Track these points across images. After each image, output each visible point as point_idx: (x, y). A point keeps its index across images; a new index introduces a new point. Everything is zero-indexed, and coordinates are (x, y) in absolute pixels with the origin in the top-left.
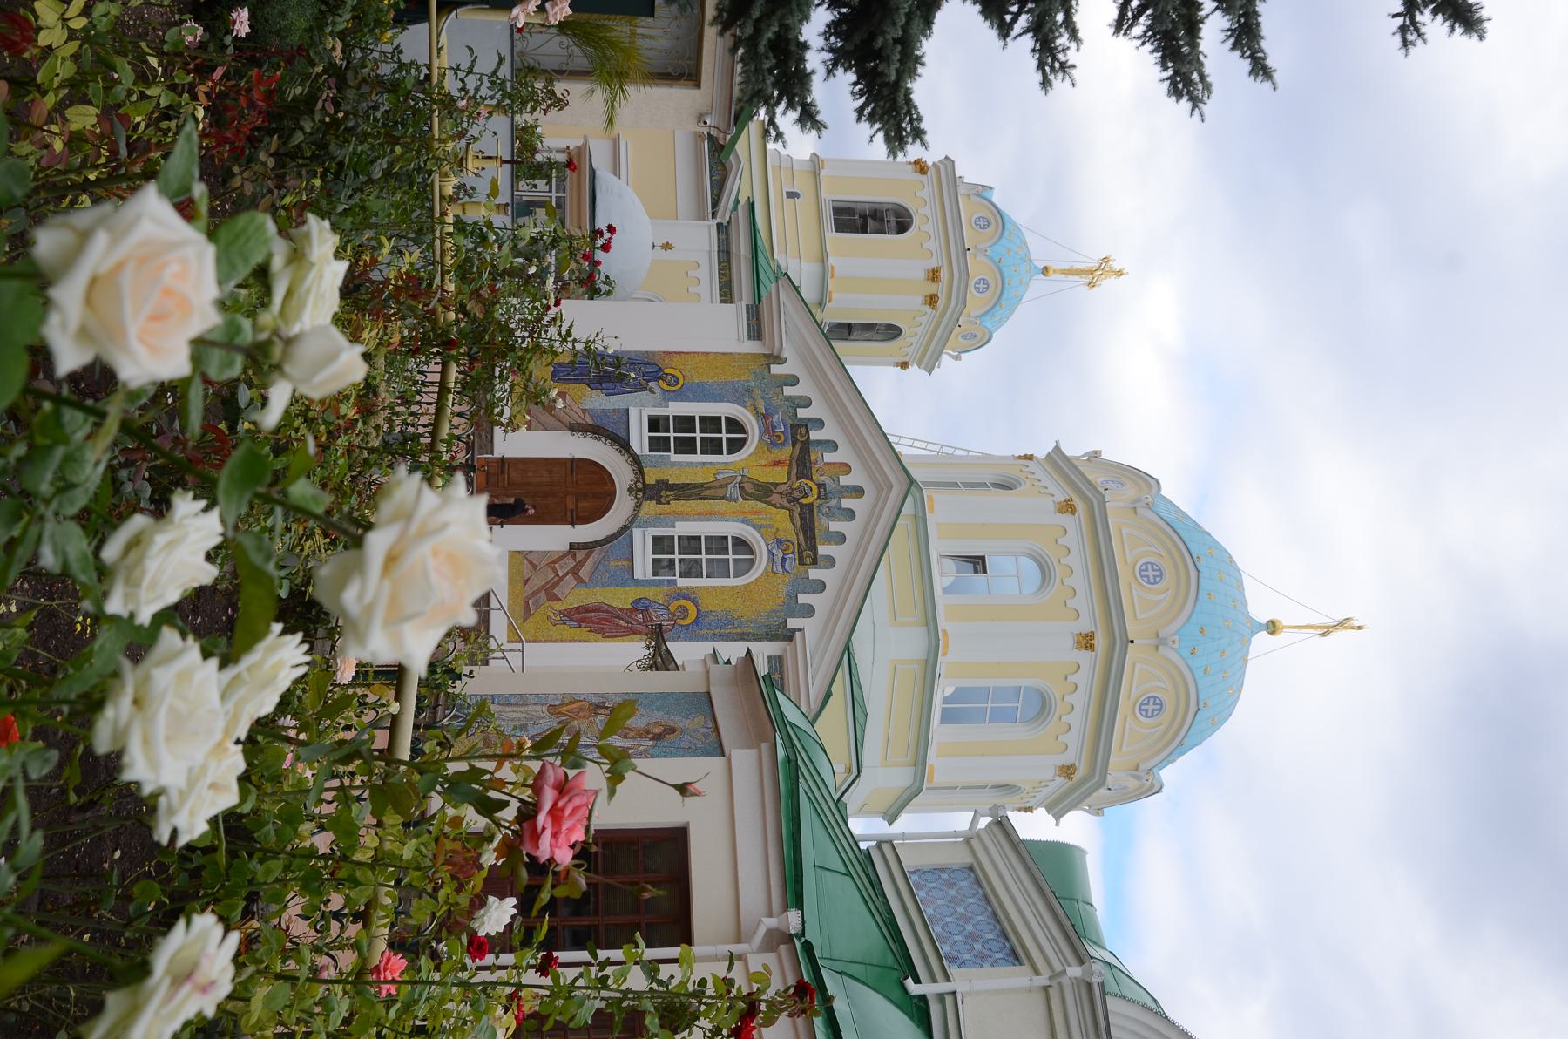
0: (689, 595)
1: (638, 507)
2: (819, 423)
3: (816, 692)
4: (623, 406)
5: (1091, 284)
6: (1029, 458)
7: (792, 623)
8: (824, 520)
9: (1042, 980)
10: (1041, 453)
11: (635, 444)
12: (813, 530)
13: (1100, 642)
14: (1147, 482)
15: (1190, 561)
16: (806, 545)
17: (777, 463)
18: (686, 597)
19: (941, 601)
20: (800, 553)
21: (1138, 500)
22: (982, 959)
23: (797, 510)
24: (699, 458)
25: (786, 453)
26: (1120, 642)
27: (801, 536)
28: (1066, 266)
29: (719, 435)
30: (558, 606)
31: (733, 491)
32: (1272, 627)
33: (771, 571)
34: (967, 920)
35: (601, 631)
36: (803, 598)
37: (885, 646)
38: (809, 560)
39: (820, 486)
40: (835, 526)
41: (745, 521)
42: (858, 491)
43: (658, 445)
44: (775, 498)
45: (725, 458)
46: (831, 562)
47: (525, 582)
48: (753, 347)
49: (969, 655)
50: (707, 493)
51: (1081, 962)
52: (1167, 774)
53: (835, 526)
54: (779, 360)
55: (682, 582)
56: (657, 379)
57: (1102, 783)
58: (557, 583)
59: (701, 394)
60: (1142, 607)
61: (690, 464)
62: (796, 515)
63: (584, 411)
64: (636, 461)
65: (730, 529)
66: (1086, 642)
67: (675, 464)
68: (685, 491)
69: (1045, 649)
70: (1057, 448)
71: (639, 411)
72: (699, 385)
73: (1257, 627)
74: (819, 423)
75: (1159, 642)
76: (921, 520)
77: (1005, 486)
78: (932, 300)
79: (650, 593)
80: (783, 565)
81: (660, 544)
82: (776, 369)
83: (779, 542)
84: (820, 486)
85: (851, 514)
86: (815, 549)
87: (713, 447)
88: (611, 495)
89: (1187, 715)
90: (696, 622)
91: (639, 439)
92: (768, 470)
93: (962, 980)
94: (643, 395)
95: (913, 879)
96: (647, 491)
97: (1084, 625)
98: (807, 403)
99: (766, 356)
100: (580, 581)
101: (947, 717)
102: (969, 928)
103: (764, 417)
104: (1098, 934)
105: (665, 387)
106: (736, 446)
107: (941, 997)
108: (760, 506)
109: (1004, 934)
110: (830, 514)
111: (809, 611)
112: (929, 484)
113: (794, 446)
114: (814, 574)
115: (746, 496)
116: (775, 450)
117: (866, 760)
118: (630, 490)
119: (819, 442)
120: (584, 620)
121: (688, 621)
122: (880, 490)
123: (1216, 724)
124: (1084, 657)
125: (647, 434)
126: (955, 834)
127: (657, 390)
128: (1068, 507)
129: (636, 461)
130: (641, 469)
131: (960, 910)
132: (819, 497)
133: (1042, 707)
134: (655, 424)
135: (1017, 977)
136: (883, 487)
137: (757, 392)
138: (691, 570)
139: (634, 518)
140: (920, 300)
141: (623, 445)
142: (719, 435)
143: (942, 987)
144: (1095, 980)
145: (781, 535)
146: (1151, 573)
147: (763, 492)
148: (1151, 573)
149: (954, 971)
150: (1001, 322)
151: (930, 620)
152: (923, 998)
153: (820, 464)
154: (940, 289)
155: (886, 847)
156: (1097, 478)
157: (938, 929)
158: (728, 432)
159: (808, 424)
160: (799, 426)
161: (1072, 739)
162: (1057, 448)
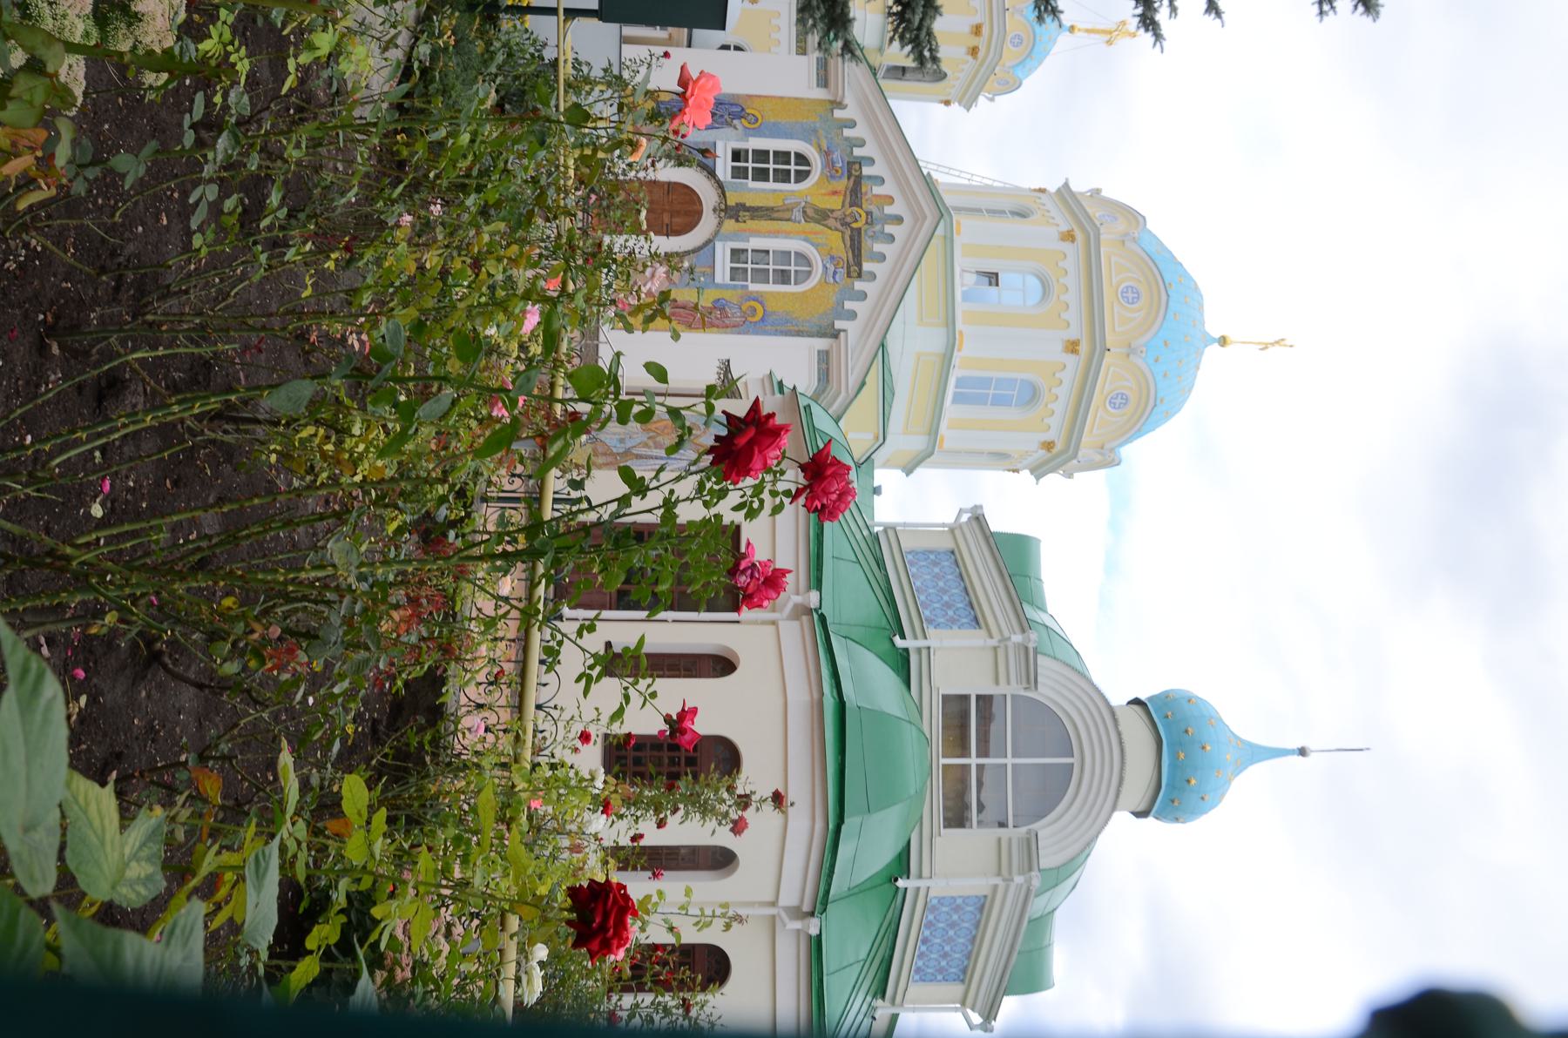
0: (758, 298)
1: (720, 224)
2: (871, 161)
3: (853, 380)
5: (1109, 42)
6: (1042, 191)
7: (839, 324)
8: (869, 242)
9: (994, 642)
10: (1052, 188)
11: (719, 173)
12: (860, 250)
13: (1084, 348)
14: (1134, 217)
15: (1161, 286)
16: (854, 262)
17: (835, 193)
19: (961, 307)
21: (1127, 234)
22: (952, 622)
24: (771, 185)
25: (843, 184)
26: (1099, 349)
28: (1089, 26)
29: (789, 167)
31: (797, 214)
32: (1223, 341)
34: (945, 591)
36: (848, 305)
37: (913, 341)
40: (878, 247)
41: (806, 240)
42: (899, 220)
43: (739, 173)
44: (831, 222)
45: (791, 186)
46: (873, 276)
48: (820, 94)
49: (978, 350)
50: (775, 215)
51: (1023, 631)
52: (1128, 451)
53: (878, 247)
54: (839, 105)
55: (753, 287)
57: (1075, 456)
59: (776, 132)
60: (1119, 321)
61: (764, 190)
64: (720, 186)
65: (793, 245)
66: (1072, 347)
67: (751, 190)
68: (757, 212)
69: (1040, 351)
70: (1066, 185)
73: (1208, 340)
74: (871, 161)
75: (1131, 351)
76: (949, 240)
77: (1022, 214)
78: (974, 51)
79: (727, 295)
81: (736, 254)
82: (838, 114)
83: (832, 258)
84: (869, 213)
85: (891, 238)
86: (860, 265)
87: (783, 176)
88: (700, 213)
89: (1145, 409)
90: (763, 320)
91: (724, 167)
93: (938, 639)
94: (728, 131)
95: (909, 558)
96: (731, 211)
97: (1073, 333)
98: (862, 143)
99: (832, 102)
101: (958, 399)
102: (946, 598)
103: (826, 154)
104: (1044, 603)
106: (802, 176)
107: (919, 650)
108: (819, 228)
109: (971, 605)
110: (874, 237)
111: (852, 315)
112: (959, 209)
114: (859, 285)
117: (891, 428)
118: (714, 210)
119: (870, 177)
121: (757, 318)
122: (916, 220)
123: (1168, 415)
124: (1070, 360)
125: (730, 164)
126: (944, 525)
128: (1069, 237)
129: (720, 186)
130: (724, 193)
131: (941, 584)
133: (1032, 395)
134: (737, 155)
135: (976, 638)
136: (919, 218)
137: (821, 132)
138: (761, 276)
139: (716, 233)
140: (963, 50)
141: (711, 173)
142: (789, 167)
143: (921, 643)
144: (1031, 646)
145: (834, 253)
146: (1130, 295)
147: (822, 216)
148: (1130, 295)
149: (930, 631)
150: (1031, 71)
151: (950, 322)
152: (906, 650)
154: (981, 42)
155: (891, 533)
156: (1095, 212)
157: (923, 598)
159: (860, 162)
161: (1054, 422)
162: (1066, 185)
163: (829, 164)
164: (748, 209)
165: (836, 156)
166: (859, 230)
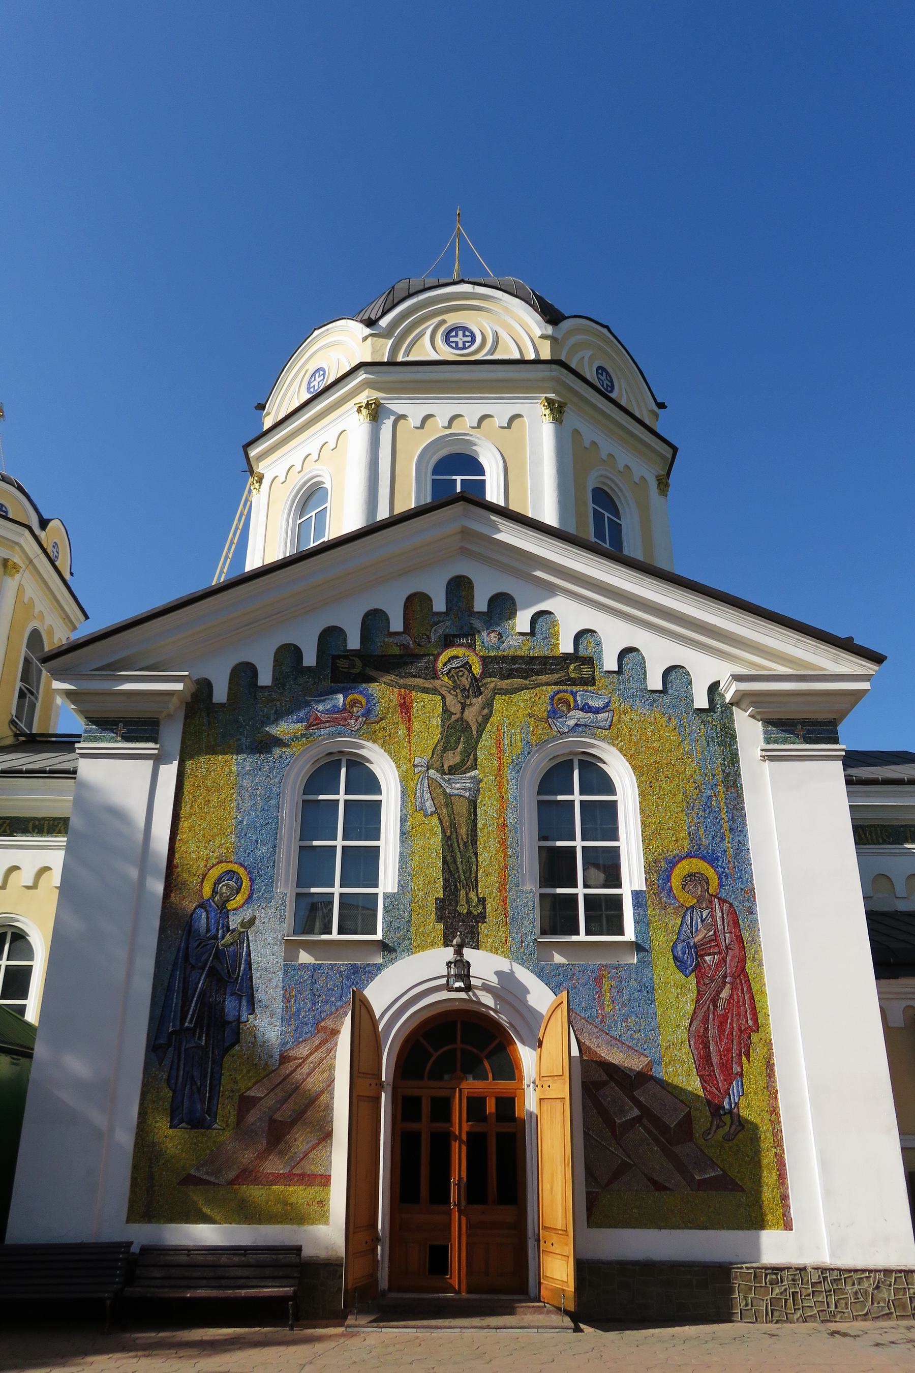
0: (659, 869)
17: (405, 707)
20: (573, 682)
23: (493, 682)
27: (543, 678)
31: (458, 786)
38: (586, 669)
44: (471, 715)
47: (659, 1187)
58: (656, 1121)
62: (505, 684)
80: (597, 711)
83: (554, 714)
90: (711, 860)
92: (416, 725)
105: (240, 898)
115: (469, 762)
120: (726, 1067)
121: (711, 873)
127: (247, 914)
145: (543, 708)
153: (408, 640)
166: (485, 660)
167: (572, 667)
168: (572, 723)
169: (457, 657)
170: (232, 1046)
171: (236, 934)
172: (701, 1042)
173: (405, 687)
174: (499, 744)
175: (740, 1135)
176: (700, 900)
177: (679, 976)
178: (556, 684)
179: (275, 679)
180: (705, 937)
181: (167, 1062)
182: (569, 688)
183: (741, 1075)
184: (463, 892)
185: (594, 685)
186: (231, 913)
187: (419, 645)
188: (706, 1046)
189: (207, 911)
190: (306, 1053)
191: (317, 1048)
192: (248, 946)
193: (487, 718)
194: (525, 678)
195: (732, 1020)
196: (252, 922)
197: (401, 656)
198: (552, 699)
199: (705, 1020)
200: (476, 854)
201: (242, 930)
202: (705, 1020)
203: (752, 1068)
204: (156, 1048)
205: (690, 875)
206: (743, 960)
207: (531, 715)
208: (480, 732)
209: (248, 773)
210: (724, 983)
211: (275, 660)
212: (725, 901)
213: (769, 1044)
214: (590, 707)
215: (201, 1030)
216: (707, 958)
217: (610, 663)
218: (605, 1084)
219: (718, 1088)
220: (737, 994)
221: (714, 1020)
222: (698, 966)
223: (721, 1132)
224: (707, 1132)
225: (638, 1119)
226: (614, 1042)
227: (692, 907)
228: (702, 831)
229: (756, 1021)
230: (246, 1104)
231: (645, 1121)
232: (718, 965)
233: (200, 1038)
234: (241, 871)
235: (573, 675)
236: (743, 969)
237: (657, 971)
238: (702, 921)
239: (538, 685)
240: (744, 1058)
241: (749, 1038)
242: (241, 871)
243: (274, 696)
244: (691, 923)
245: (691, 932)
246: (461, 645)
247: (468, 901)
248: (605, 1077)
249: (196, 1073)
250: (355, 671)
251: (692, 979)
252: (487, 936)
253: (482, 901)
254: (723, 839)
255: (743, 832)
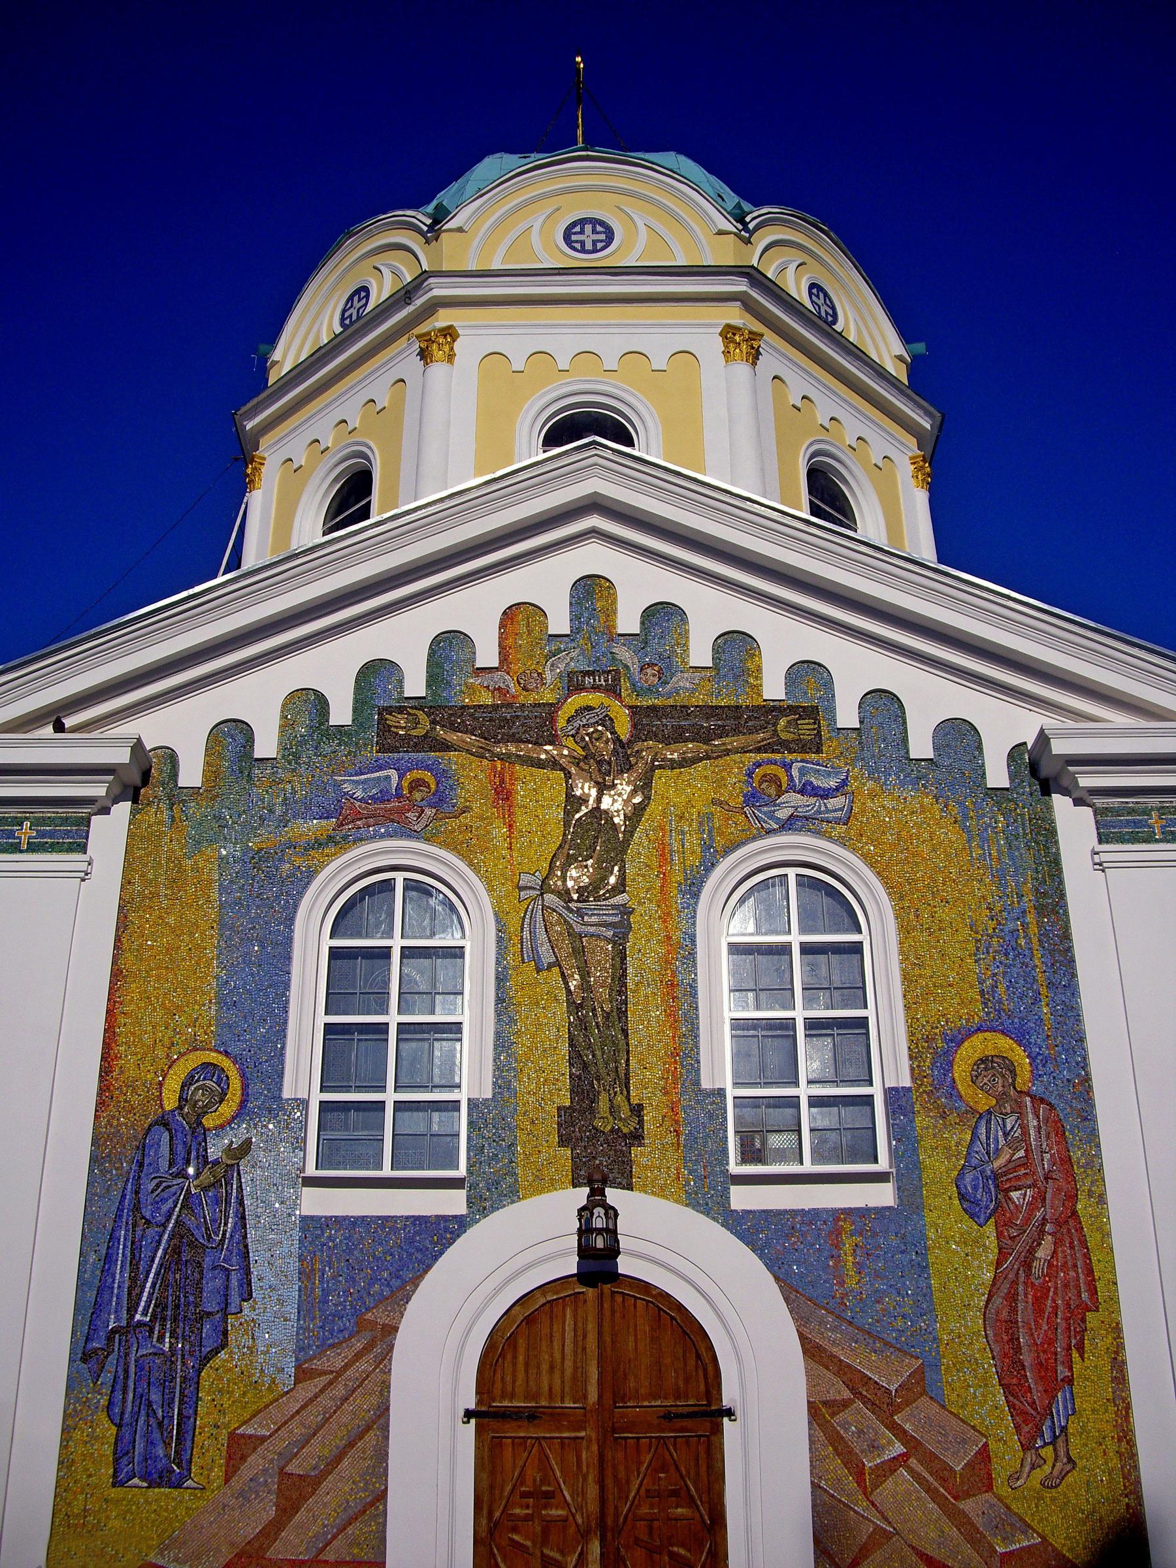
0: (933, 1049)
4: (290, 1244)
8: (681, 681)
12: (711, 711)
17: (503, 794)
18: (945, 1061)
20: (786, 746)
23: (648, 749)
27: (734, 742)
30: (1007, 1452)
33: (845, 828)
35: (1078, 1314)
36: (921, 746)
38: (806, 726)
39: (574, 683)
40: (700, 654)
41: (693, 888)
42: (591, 592)
48: (110, 832)
56: (199, 1133)
58: (929, 1459)
63: (303, 1374)
71: (295, 1195)
72: (221, 1002)
80: (826, 794)
86: (774, 710)
100: (919, 1385)
105: (227, 1109)
108: (641, 846)
113: (446, 747)
114: (847, 716)
116: (460, 797)
120: (1045, 1370)
121: (1020, 1056)
132: (613, 690)
158: (389, 934)
160: (384, 729)
163: (390, 814)
164: (584, 1091)
165: (354, 787)
167: (782, 722)
168: (783, 814)
169: (589, 708)
170: (216, 1351)
171: (220, 1171)
172: (1004, 1332)
173: (500, 757)
174: (664, 854)
175: (1070, 1479)
176: (1001, 1098)
177: (967, 1224)
178: (758, 750)
179: (283, 747)
180: (1010, 1161)
181: (107, 1377)
182: (778, 757)
183: (1070, 1381)
184: (603, 1099)
185: (819, 751)
186: (210, 1135)
187: (525, 689)
188: (1014, 1340)
189: (169, 1130)
190: (339, 1364)
191: (358, 1356)
192: (240, 1187)
193: (639, 810)
194: (707, 741)
195: (1055, 1293)
196: (246, 1147)
197: (495, 707)
198: (750, 775)
199: (1012, 1297)
200: (625, 1032)
201: (229, 1162)
202: (1012, 1297)
203: (1088, 1368)
204: (88, 1353)
205: (985, 1061)
206: (1073, 1197)
207: (714, 802)
208: (630, 833)
209: (238, 902)
210: (1042, 1232)
211: (284, 717)
212: (1042, 1100)
213: (1117, 1330)
214: (814, 788)
215: (163, 1326)
216: (1015, 1195)
217: (847, 716)
218: (845, 1404)
219: (1033, 1404)
220: (1063, 1252)
221: (1026, 1295)
222: (998, 1205)
223: (1039, 1474)
224: (1014, 1477)
225: (904, 1457)
226: (860, 1336)
227: (989, 1112)
228: (1001, 989)
229: (1093, 1292)
230: (239, 1448)
231: (913, 1462)
232: (1032, 1207)
233: (161, 1339)
234: (226, 1063)
235: (784, 736)
236: (1074, 1213)
237: (929, 1217)
238: (1006, 1134)
239: (727, 752)
240: (1075, 1355)
241: (1083, 1320)
242: (226, 1063)
243: (281, 774)
244: (988, 1138)
245: (988, 1153)
246: (595, 688)
247: (613, 1110)
248: (847, 1394)
249: (155, 1397)
250: (414, 733)
251: (990, 1229)
252: (646, 1167)
253: (637, 1110)
254: (1036, 1001)
255: (1071, 988)
